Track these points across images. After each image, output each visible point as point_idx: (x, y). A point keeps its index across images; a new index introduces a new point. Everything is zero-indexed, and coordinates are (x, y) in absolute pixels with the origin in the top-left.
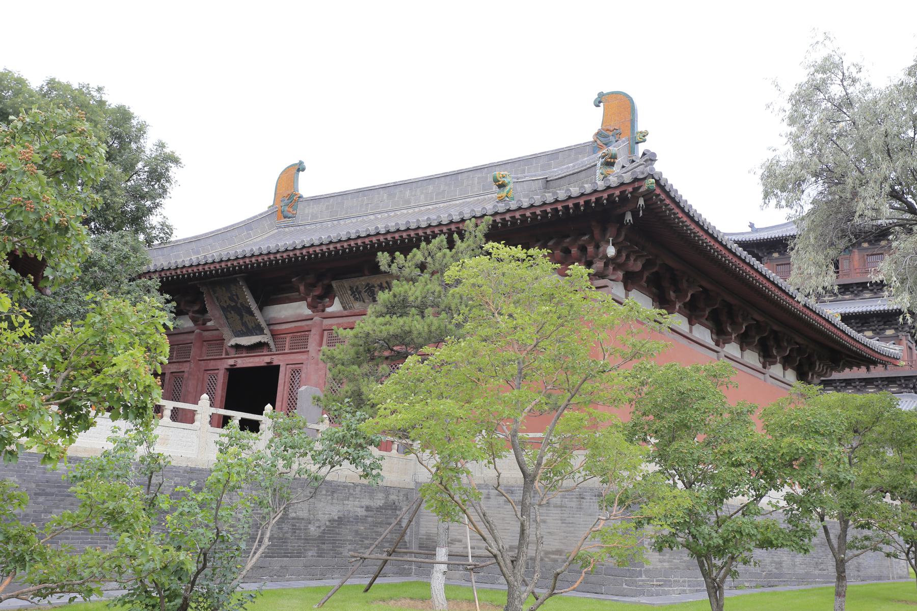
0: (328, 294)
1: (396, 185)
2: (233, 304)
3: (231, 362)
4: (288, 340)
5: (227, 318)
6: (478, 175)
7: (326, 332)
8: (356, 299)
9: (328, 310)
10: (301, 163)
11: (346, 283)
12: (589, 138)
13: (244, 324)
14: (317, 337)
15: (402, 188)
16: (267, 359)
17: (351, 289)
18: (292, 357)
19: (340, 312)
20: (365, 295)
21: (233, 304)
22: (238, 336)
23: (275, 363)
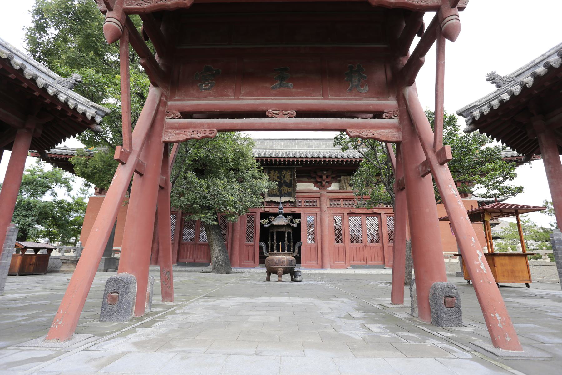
1: (264, 139)
6: (305, 142)
9: (328, 189)
15: (268, 141)
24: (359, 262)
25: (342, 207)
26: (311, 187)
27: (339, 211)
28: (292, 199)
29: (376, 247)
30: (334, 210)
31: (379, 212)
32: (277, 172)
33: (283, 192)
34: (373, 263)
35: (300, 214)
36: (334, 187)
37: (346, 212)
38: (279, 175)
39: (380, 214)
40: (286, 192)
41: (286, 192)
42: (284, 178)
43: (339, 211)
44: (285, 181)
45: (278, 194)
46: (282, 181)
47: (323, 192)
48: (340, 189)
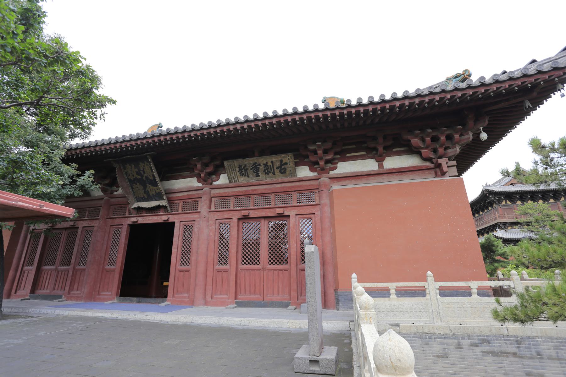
0: (216, 172)
2: (139, 177)
3: (134, 219)
4: (181, 204)
5: (132, 188)
7: (213, 199)
8: (242, 175)
9: (215, 183)
10: (160, 124)
11: (236, 163)
13: (147, 193)
14: (208, 202)
16: (165, 218)
17: (240, 167)
20: (250, 172)
21: (139, 177)
22: (140, 201)
23: (171, 220)
24: (252, 296)
25: (232, 208)
26: (193, 182)
27: (226, 215)
28: (163, 203)
29: (280, 270)
30: (218, 214)
31: (286, 213)
32: (133, 166)
33: (151, 194)
34: (275, 298)
35: (173, 223)
36: (223, 179)
37: (235, 216)
38: (137, 170)
39: (289, 216)
40: (154, 193)
41: (154, 193)
42: (144, 173)
43: (226, 215)
44: (147, 177)
45: (146, 197)
46: (144, 178)
47: (206, 189)
48: (230, 182)
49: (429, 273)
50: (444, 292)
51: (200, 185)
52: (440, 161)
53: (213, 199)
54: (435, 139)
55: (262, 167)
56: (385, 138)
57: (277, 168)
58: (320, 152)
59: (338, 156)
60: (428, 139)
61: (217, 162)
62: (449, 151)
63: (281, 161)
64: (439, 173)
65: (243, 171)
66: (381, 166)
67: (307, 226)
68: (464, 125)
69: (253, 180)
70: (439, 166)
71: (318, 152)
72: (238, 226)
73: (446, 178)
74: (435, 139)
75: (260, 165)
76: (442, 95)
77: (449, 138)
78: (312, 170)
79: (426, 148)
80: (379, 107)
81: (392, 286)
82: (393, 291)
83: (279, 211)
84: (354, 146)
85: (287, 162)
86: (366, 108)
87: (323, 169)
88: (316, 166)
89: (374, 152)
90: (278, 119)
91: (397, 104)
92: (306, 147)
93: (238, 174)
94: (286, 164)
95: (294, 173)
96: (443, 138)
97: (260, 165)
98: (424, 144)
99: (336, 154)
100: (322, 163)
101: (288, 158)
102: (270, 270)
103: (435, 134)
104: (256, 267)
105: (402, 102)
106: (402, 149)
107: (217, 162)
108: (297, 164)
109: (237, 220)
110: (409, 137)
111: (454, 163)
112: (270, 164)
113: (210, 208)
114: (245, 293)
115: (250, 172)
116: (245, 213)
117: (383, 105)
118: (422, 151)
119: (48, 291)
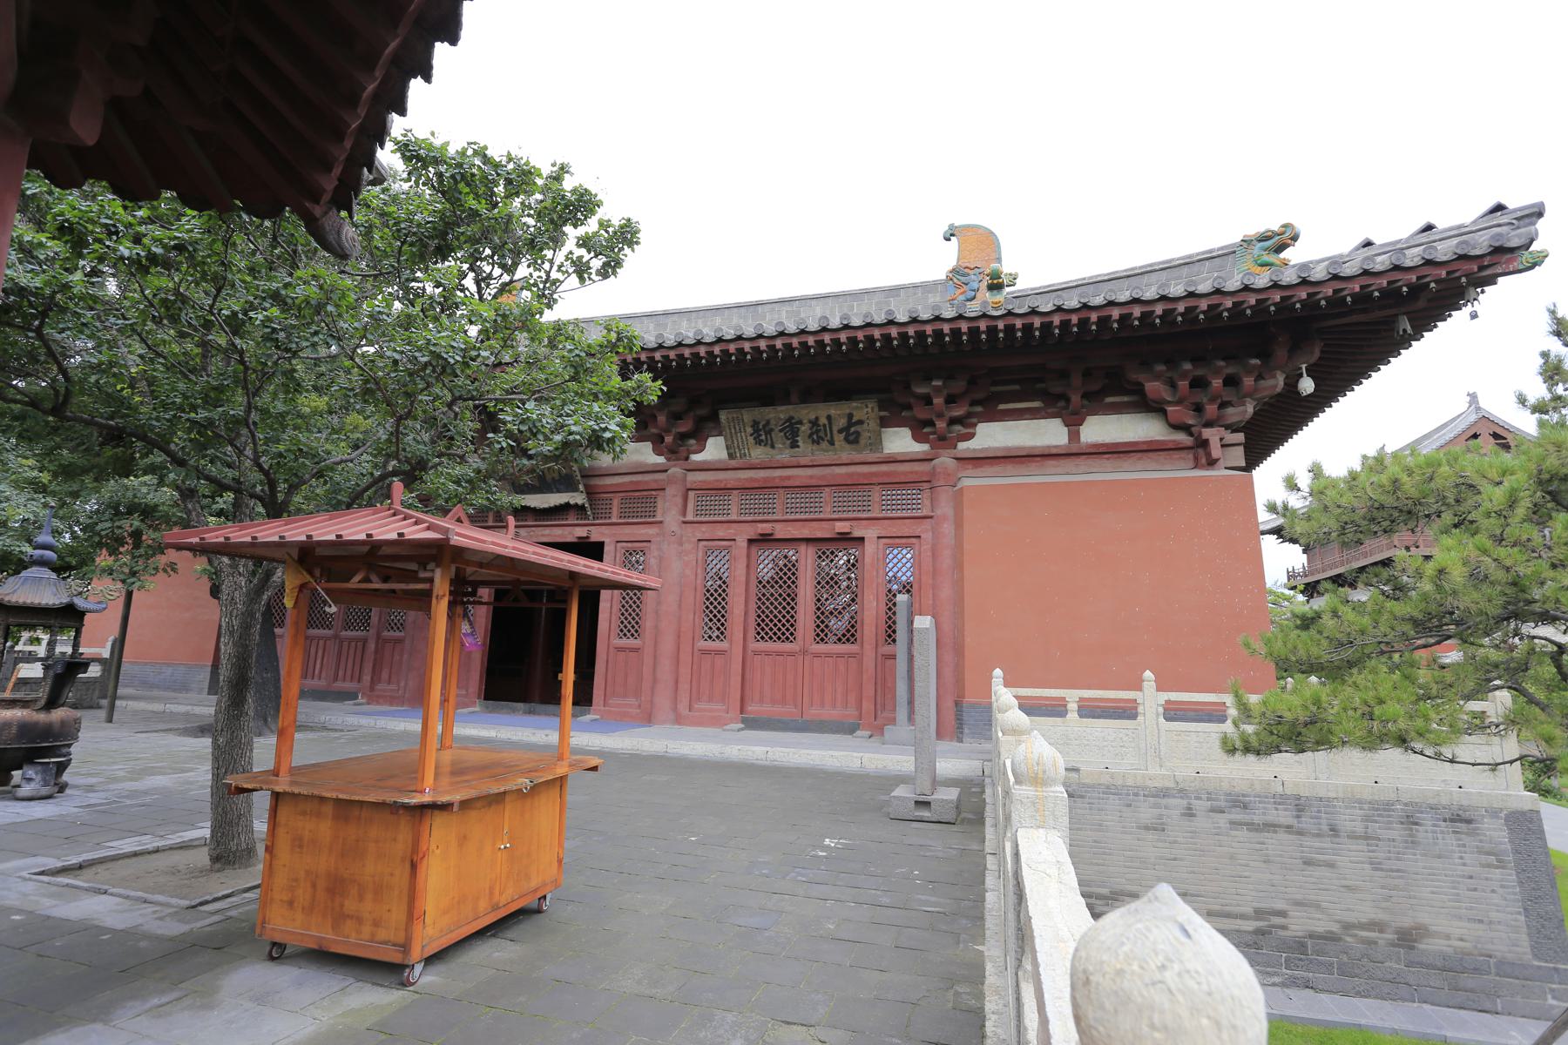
0: (699, 435)
1: (666, 314)
4: (616, 502)
6: (787, 308)
7: (691, 494)
8: (759, 442)
9: (695, 457)
11: (748, 415)
12: (941, 275)
14: (679, 500)
15: (675, 317)
17: (755, 424)
18: (627, 530)
19: (720, 461)
20: (778, 436)
22: (523, 492)
23: (595, 538)
24: (778, 709)
25: (734, 517)
27: (721, 532)
28: (578, 498)
29: (840, 656)
30: (704, 527)
31: (857, 533)
35: (601, 544)
36: (714, 449)
37: (743, 534)
39: (862, 539)
40: (556, 476)
41: (556, 476)
43: (721, 532)
47: (676, 470)
48: (731, 456)
49: (1148, 674)
50: (1174, 713)
51: (661, 460)
52: (1207, 433)
53: (691, 494)
54: (1199, 383)
55: (805, 428)
56: (1087, 374)
57: (840, 431)
58: (938, 401)
59: (979, 409)
60: (1183, 384)
61: (702, 412)
62: (1230, 410)
63: (850, 416)
64: (1204, 461)
65: (762, 434)
66: (1074, 436)
67: (901, 564)
68: (1265, 355)
69: (784, 455)
70: (1204, 444)
71: (935, 401)
72: (748, 556)
73: (1218, 472)
74: (1199, 383)
75: (800, 422)
76: (1215, 300)
77: (1231, 382)
78: (917, 438)
79: (1178, 403)
80: (1074, 319)
81: (1072, 696)
82: (1072, 706)
83: (841, 527)
84: (1017, 387)
85: (864, 418)
86: (1047, 319)
87: (942, 438)
88: (926, 430)
89: (1062, 404)
90: (852, 334)
91: (1116, 313)
92: (907, 387)
93: (751, 440)
94: (860, 422)
95: (877, 443)
96: (1217, 383)
97: (800, 422)
98: (1174, 394)
99: (973, 403)
100: (941, 425)
101: (866, 410)
102: (817, 655)
103: (1199, 372)
104: (787, 646)
105: (1125, 311)
106: (1126, 399)
107: (702, 412)
108: (885, 423)
109: (745, 544)
110: (1141, 377)
111: (1240, 437)
112: (823, 421)
113: (684, 514)
114: (761, 701)
115: (778, 436)
116: (765, 528)
117: (1083, 314)
118: (1169, 409)
119: (323, 683)
